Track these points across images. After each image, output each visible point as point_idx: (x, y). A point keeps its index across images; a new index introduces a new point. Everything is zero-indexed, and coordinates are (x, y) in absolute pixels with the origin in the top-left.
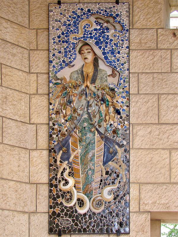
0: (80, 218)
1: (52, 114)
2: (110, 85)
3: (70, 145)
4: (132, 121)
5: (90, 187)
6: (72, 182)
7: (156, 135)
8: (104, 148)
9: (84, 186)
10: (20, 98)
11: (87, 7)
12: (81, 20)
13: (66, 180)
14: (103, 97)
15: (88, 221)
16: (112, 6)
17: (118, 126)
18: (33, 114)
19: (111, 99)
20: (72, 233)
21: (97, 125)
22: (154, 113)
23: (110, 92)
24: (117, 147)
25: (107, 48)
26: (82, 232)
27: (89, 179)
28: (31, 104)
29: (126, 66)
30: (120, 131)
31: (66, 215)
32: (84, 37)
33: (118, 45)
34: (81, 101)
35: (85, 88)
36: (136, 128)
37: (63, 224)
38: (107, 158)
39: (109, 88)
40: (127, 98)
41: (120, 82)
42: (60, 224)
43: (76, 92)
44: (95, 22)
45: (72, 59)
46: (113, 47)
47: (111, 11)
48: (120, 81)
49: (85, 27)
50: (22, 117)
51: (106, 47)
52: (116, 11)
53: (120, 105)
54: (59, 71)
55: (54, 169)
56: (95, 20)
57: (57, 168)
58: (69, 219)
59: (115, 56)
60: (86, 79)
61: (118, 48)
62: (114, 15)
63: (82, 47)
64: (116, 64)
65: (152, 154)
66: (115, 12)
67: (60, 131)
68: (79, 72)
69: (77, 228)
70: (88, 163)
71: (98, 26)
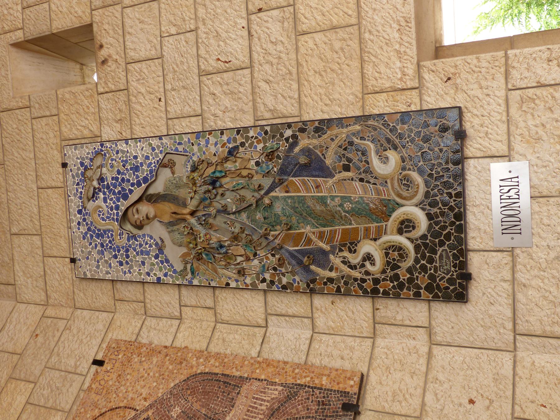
0: (437, 228)
1: (245, 283)
3: (299, 248)
4: (249, 123)
7: (272, 71)
9: (372, 219)
10: (221, 341)
11: (75, 216)
13: (364, 260)
16: (71, 174)
17: (258, 149)
18: (248, 320)
19: (212, 167)
21: (259, 194)
22: (233, 79)
27: (359, 209)
28: (233, 322)
29: (155, 142)
31: (431, 261)
33: (124, 159)
36: (262, 112)
37: (448, 267)
40: (208, 136)
41: (181, 152)
43: (201, 235)
44: (95, 202)
45: (152, 241)
47: (77, 175)
49: (103, 219)
50: (255, 342)
51: (128, 181)
52: (76, 167)
53: (221, 149)
54: (173, 267)
57: (343, 277)
58: (439, 253)
59: (142, 164)
60: (179, 216)
62: (82, 169)
64: (154, 161)
65: (309, 73)
66: (78, 169)
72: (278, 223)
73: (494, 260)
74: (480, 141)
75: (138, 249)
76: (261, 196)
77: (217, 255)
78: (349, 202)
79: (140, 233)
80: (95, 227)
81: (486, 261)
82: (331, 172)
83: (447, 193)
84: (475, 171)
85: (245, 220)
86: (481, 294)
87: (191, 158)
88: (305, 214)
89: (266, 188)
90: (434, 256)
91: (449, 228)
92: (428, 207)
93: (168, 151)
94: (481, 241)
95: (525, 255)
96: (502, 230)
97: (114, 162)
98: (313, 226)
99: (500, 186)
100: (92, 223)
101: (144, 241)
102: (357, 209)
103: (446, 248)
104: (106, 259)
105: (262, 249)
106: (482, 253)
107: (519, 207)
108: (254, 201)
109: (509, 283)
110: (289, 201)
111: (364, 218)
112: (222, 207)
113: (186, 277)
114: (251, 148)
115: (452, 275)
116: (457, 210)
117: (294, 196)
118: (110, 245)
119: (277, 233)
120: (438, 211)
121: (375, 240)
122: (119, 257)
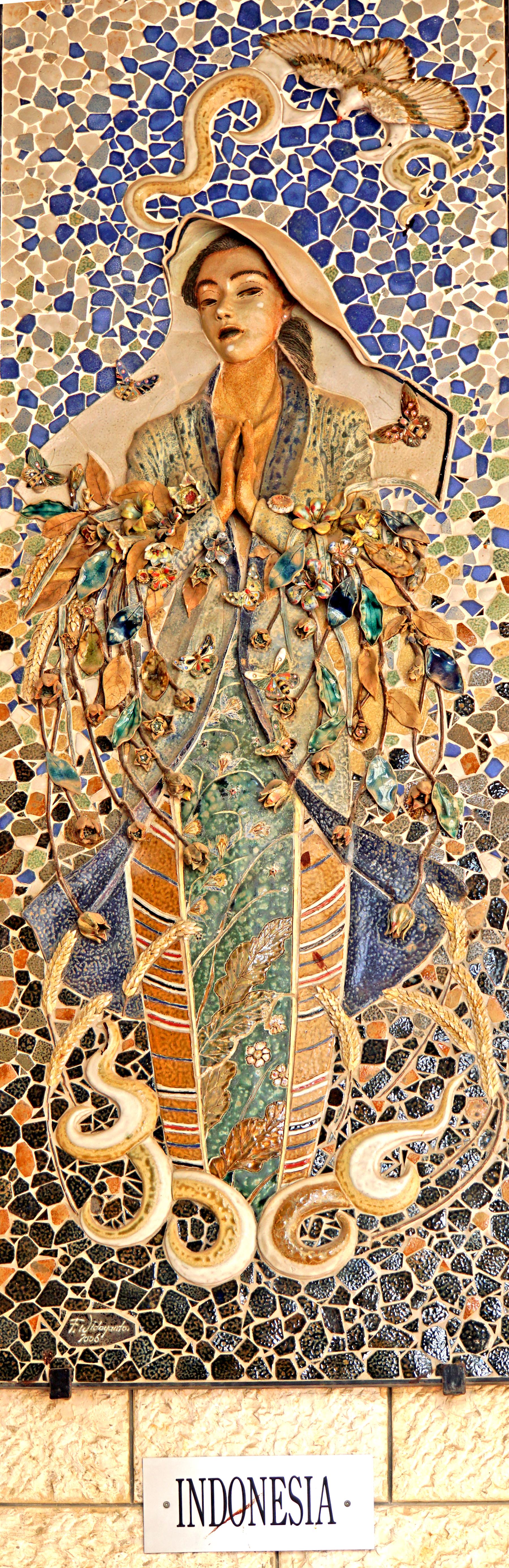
2: (390, 497)
5: (261, 1138)
6: (140, 1111)
8: (354, 907)
9: (219, 1128)
12: (199, 81)
13: (99, 1100)
14: (342, 584)
15: (246, 1323)
17: (445, 761)
19: (395, 592)
20: (141, 1380)
23: (386, 539)
24: (436, 894)
25: (366, 254)
26: (210, 1379)
27: (250, 1089)
30: (459, 795)
32: (217, 191)
34: (198, 610)
35: (227, 524)
37: (84, 1338)
38: (372, 963)
39: (382, 518)
41: (454, 470)
42: (59, 1339)
44: (287, 88)
45: (144, 343)
46: (409, 246)
48: (454, 465)
49: (221, 125)
51: (360, 244)
53: (453, 624)
55: (26, 1043)
56: (289, 71)
61: (436, 248)
63: (203, 257)
67: (62, 812)
68: (188, 424)
69: (177, 1358)
70: (243, 998)
71: (310, 108)
72: (207, 828)
73: (106, 1459)
74: (437, 1429)
75: (115, 281)
76: (293, 775)
77: (100, 601)
78: (271, 1060)
79: (174, 293)
80: (191, 89)
81: (105, 1438)
82: (361, 1003)
83: (291, 1340)
84: (352, 1415)
85: (219, 713)
86: (12, 1423)
87: (430, 510)
88: (234, 920)
89: (318, 789)
90: (115, 1300)
91: (194, 1344)
92: (252, 1287)
93: (456, 416)
94: (160, 1425)
95: (124, 1535)
96: (190, 1481)
97: (432, 177)
98: (199, 943)
99: (309, 1479)
100: (209, 71)
101: (143, 307)
102: (248, 1083)
103: (138, 1335)
104: (76, 135)
105: (126, 770)
106: (126, 1426)
107: (252, 1524)
108: (277, 750)
109: (45, 1494)
110: (276, 868)
111: (223, 1103)
112: (260, 635)
113: (22, 484)
114: (450, 736)
115: (63, 1349)
116: (245, 1365)
117: (291, 883)
118: (127, 154)
119: (177, 823)
120: (242, 1315)
121: (158, 1134)
122: (84, 194)
